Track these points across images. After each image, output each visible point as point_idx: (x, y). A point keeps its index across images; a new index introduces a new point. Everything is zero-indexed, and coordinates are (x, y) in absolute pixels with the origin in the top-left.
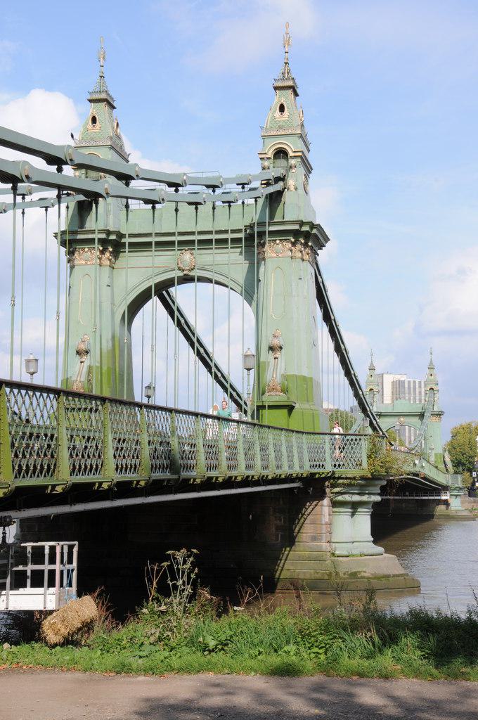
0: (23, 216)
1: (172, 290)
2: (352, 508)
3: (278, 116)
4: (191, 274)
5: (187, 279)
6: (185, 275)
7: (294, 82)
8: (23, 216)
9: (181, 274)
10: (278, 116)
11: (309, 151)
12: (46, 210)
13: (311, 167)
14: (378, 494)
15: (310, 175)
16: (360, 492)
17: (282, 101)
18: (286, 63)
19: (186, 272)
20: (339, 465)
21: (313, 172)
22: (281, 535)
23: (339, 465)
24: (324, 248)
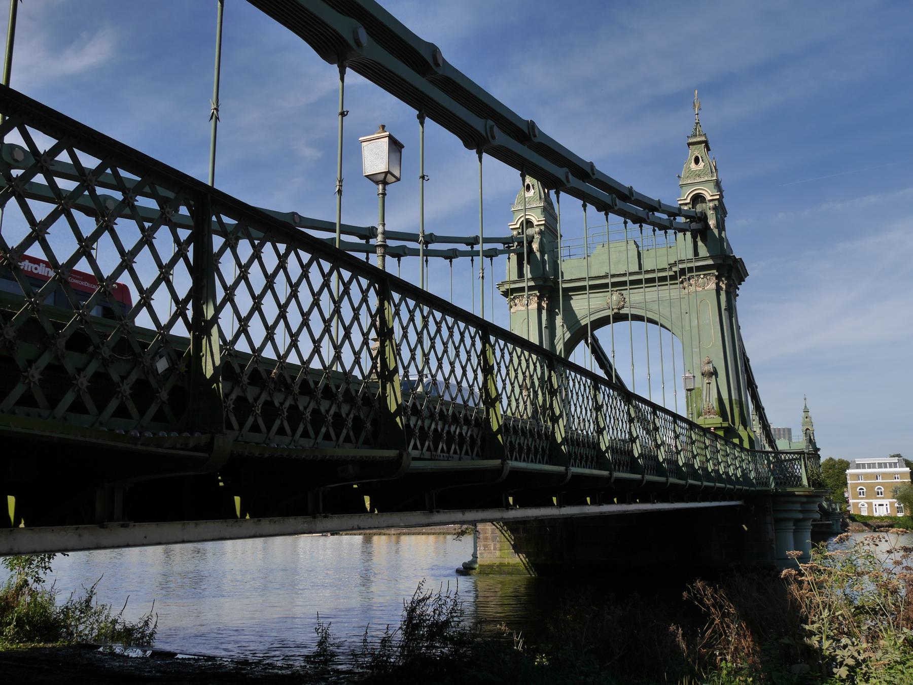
0: (472, 263)
4: (621, 312)
8: (472, 263)
15: (725, 218)
16: (800, 509)
17: (696, 154)
18: (697, 123)
19: (616, 311)
23: (781, 483)
24: (742, 283)
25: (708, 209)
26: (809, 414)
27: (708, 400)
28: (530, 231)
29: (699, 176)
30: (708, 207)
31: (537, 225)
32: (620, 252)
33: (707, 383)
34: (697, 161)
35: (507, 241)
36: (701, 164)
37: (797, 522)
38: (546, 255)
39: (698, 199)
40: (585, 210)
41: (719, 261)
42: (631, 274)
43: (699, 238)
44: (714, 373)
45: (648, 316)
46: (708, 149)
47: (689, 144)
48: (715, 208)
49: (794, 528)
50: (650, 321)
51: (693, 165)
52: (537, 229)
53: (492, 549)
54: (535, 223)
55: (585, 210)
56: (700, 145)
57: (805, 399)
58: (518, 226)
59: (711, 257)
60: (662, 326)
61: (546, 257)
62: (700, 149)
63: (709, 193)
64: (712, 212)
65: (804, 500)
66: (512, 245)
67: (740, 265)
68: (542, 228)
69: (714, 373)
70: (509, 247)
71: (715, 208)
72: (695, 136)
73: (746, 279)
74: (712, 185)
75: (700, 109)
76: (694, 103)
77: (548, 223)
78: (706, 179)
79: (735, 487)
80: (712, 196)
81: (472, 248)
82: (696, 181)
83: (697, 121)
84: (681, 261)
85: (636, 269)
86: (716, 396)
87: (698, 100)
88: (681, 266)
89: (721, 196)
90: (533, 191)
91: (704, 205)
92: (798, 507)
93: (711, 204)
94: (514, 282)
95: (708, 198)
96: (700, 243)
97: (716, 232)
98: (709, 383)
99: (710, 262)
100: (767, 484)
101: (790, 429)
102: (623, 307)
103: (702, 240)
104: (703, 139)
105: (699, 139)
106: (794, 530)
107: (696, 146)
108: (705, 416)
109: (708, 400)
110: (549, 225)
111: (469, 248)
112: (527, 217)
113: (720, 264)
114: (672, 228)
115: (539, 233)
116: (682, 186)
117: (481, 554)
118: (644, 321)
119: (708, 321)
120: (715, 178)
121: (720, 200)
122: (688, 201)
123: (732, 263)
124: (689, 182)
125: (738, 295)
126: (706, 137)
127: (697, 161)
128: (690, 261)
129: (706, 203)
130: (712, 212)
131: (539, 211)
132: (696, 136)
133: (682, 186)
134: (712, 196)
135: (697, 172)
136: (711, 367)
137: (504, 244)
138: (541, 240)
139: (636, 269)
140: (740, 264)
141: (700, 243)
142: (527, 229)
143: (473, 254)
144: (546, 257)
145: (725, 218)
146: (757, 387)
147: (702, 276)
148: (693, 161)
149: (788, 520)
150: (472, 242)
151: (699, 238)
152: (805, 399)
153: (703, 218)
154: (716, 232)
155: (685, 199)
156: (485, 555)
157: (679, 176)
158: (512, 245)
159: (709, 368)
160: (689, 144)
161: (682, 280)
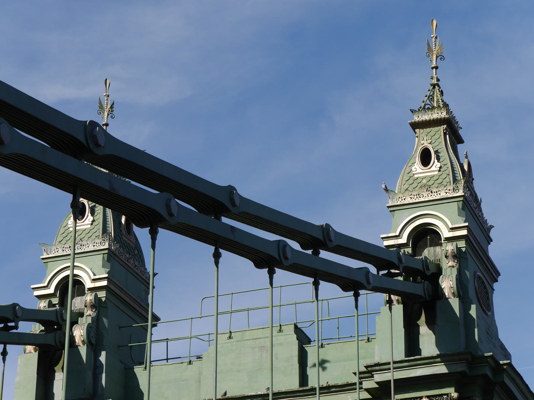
3: (419, 170)
7: (448, 112)
11: (489, 240)
15: (495, 285)
18: (434, 86)
21: (500, 279)
25: (444, 256)
29: (428, 188)
30: (444, 252)
31: (90, 289)
32: (262, 348)
36: (435, 165)
38: (103, 353)
40: (217, 263)
41: (460, 368)
43: (423, 318)
47: (415, 126)
48: (458, 255)
51: (417, 168)
52: (89, 297)
54: (88, 284)
55: (217, 263)
56: (436, 129)
58: (51, 290)
59: (443, 358)
61: (103, 358)
62: (437, 136)
64: (451, 263)
66: (13, 324)
67: (513, 380)
68: (102, 294)
71: (458, 255)
72: (424, 109)
74: (454, 207)
75: (440, 57)
76: (429, 45)
77: (116, 285)
78: (443, 195)
80: (453, 229)
82: (422, 199)
83: (434, 81)
84: (381, 367)
87: (438, 39)
88: (379, 377)
90: (91, 218)
91: (438, 249)
93: (450, 247)
95: (445, 233)
96: (424, 330)
97: (455, 303)
99: (441, 369)
103: (430, 324)
104: (443, 114)
105: (435, 115)
107: (428, 130)
110: (116, 285)
112: (76, 272)
113: (463, 374)
114: (286, 263)
115: (93, 306)
116: (393, 209)
120: (461, 193)
122: (403, 240)
123: (489, 373)
124: (408, 200)
126: (448, 112)
128: (399, 365)
129: (441, 245)
130: (451, 263)
131: (99, 259)
132: (433, 108)
133: (393, 209)
134: (453, 229)
135: (424, 181)
138: (96, 321)
140: (509, 375)
141: (424, 330)
142: (73, 298)
144: (103, 358)
151: (423, 318)
154: (455, 303)
157: (386, 190)
158: (13, 324)
160: (415, 126)
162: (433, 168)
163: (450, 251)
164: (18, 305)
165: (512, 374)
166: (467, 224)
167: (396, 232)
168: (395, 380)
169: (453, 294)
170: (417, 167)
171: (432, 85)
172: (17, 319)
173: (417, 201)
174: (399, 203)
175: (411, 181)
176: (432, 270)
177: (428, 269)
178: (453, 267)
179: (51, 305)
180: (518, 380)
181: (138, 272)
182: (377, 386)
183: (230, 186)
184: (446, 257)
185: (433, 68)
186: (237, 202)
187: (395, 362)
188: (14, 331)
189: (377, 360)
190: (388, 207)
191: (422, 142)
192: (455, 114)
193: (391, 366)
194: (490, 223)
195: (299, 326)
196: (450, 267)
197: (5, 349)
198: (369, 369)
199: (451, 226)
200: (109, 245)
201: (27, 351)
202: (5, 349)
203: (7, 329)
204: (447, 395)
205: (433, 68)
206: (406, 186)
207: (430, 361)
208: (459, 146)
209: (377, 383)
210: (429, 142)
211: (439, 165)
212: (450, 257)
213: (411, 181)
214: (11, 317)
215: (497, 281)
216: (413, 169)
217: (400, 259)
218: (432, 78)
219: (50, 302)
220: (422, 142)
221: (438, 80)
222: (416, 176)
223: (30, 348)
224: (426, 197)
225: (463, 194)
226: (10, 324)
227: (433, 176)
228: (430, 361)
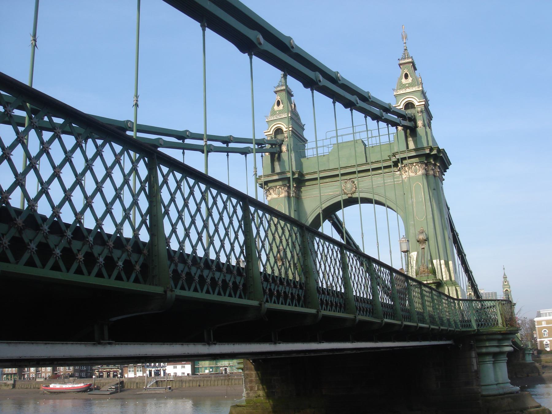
0: (228, 158)
1: (339, 213)
2: (493, 358)
4: (355, 196)
5: (351, 201)
6: (349, 197)
8: (228, 158)
9: (345, 197)
10: (404, 81)
12: (246, 156)
13: (432, 116)
14: (511, 346)
15: (431, 121)
17: (406, 71)
18: (405, 50)
19: (350, 195)
20: (482, 324)
21: (433, 119)
22: (529, 347)
23: (482, 324)
24: (447, 170)
25: (417, 112)
26: (507, 279)
27: (423, 262)
28: (279, 137)
33: (422, 249)
34: (406, 76)
35: (260, 143)
36: (410, 79)
37: (495, 355)
39: (410, 105)
42: (359, 165)
44: (427, 240)
45: (375, 199)
46: (415, 69)
47: (400, 65)
48: (421, 112)
49: (493, 360)
50: (378, 203)
51: (404, 81)
53: (256, 389)
56: (409, 65)
57: (504, 269)
58: (271, 133)
60: (388, 207)
63: (417, 102)
64: (420, 114)
65: (500, 337)
66: (264, 146)
69: (427, 240)
70: (262, 147)
73: (450, 167)
74: (419, 94)
77: (294, 129)
79: (439, 328)
80: (419, 102)
81: (227, 145)
83: (405, 48)
85: (364, 162)
86: (429, 258)
89: (427, 101)
92: (495, 343)
93: (419, 109)
94: (268, 176)
98: (424, 248)
100: (470, 326)
101: (496, 292)
102: (355, 192)
104: (410, 60)
105: (407, 61)
106: (493, 361)
108: (421, 275)
109: (423, 262)
111: (225, 145)
117: (248, 394)
118: (372, 203)
119: (421, 200)
120: (421, 89)
121: (426, 106)
125: (444, 180)
126: (412, 59)
127: (406, 76)
131: (286, 120)
134: (419, 102)
136: (425, 236)
137: (258, 144)
139: (364, 162)
143: (228, 151)
145: (431, 121)
146: (465, 255)
147: (415, 164)
148: (404, 77)
149: (488, 354)
150: (226, 140)
152: (504, 269)
153: (413, 119)
155: (399, 106)
156: (251, 395)
158: (264, 146)
159: (421, 237)
161: (400, 169)
162: (410, 80)
163: (419, 110)
164: (265, 139)
165: (444, 152)
166: (424, 100)
167: (398, 104)
168: (408, 157)
169: (422, 125)
170: (404, 80)
171: (404, 50)
172: (265, 143)
173: (405, 92)
174: (398, 94)
175: (401, 85)
176: (414, 118)
177: (413, 117)
178: (420, 116)
179: (272, 138)
180: (445, 155)
181: (300, 124)
182: (397, 160)
183: (368, 92)
184: (418, 112)
185: (404, 43)
186: (371, 97)
187: (400, 152)
188: (265, 148)
189: (396, 150)
190: (394, 95)
191: (405, 71)
192: (414, 60)
193: (406, 152)
194: (428, 99)
195: (363, 140)
196: (420, 116)
197: (262, 154)
198: (394, 154)
199: (418, 101)
200: (290, 115)
201: (266, 155)
202: (262, 154)
203: (262, 147)
204: (423, 162)
205: (404, 43)
206: (400, 87)
207: (411, 151)
208: (415, 71)
209: (397, 159)
210: (407, 70)
211: (412, 79)
212: (419, 112)
213: (401, 85)
214: (264, 143)
215: (432, 120)
216: (402, 81)
217: (406, 114)
218: (404, 47)
219: (271, 137)
220: (405, 71)
221: (407, 48)
222: (403, 83)
223: (267, 154)
224: (408, 90)
225: (422, 89)
226: (263, 146)
227: (410, 83)
228: (411, 151)
